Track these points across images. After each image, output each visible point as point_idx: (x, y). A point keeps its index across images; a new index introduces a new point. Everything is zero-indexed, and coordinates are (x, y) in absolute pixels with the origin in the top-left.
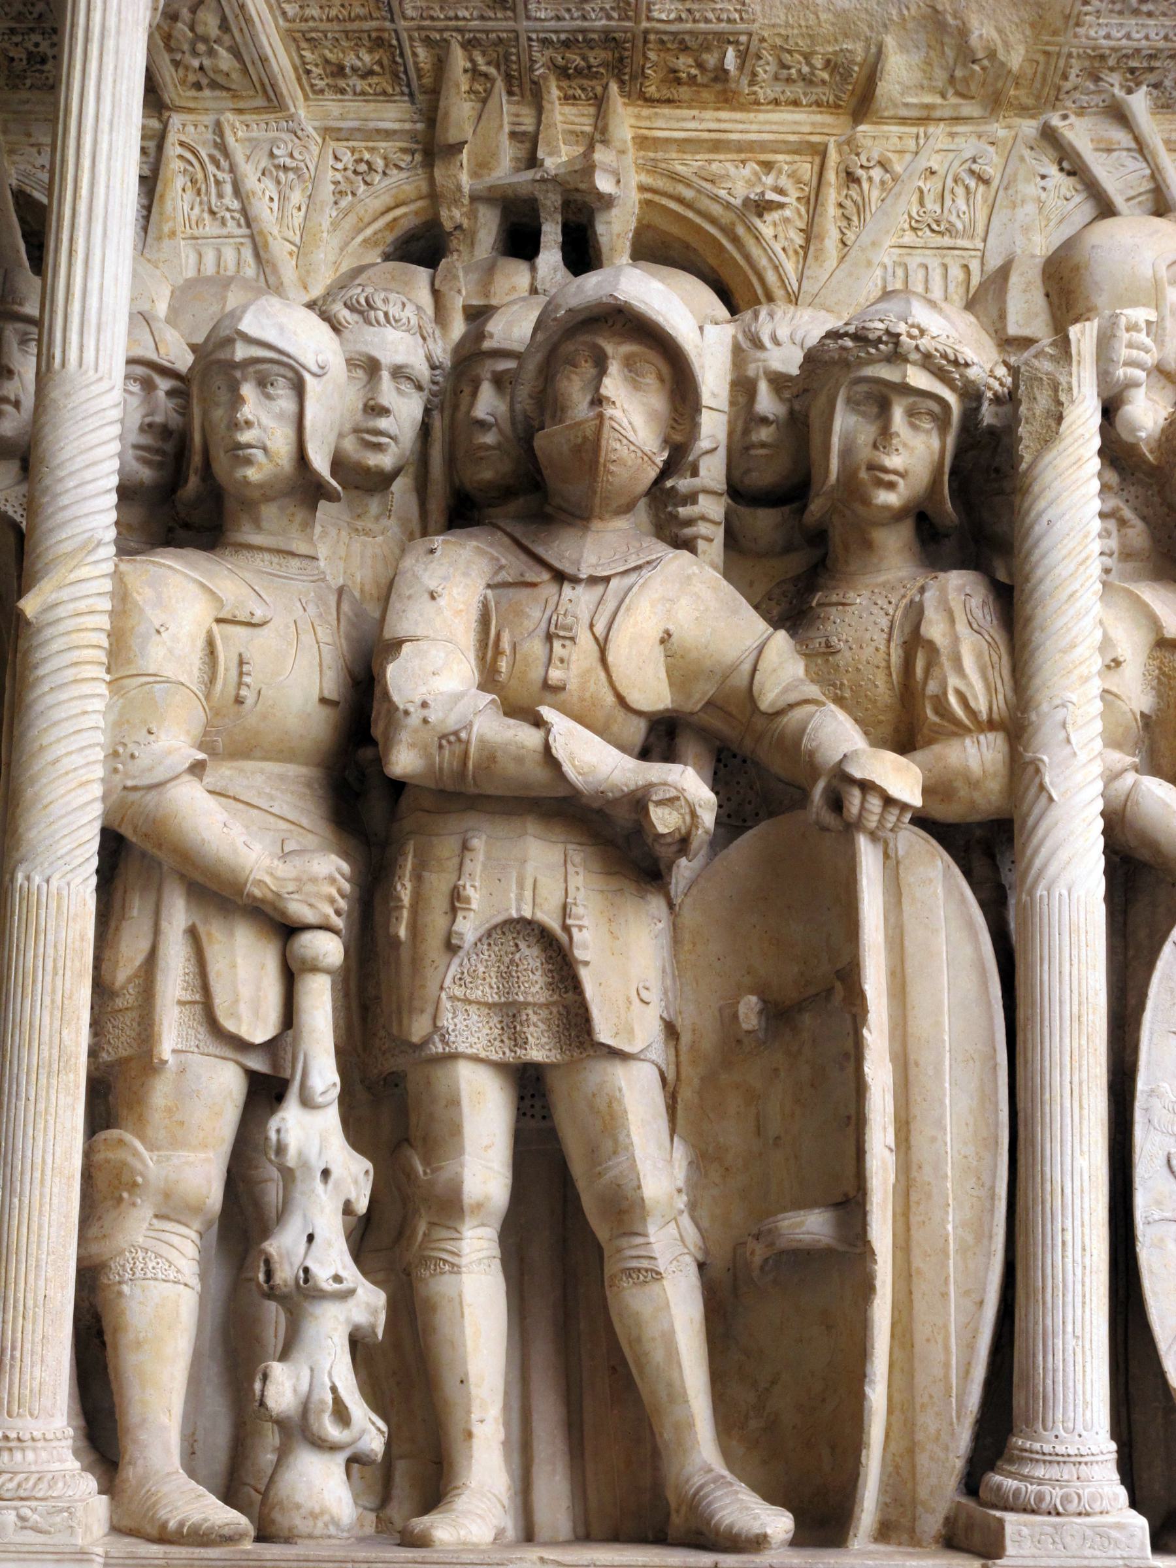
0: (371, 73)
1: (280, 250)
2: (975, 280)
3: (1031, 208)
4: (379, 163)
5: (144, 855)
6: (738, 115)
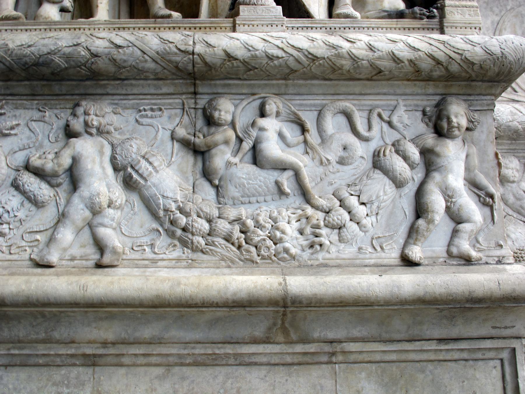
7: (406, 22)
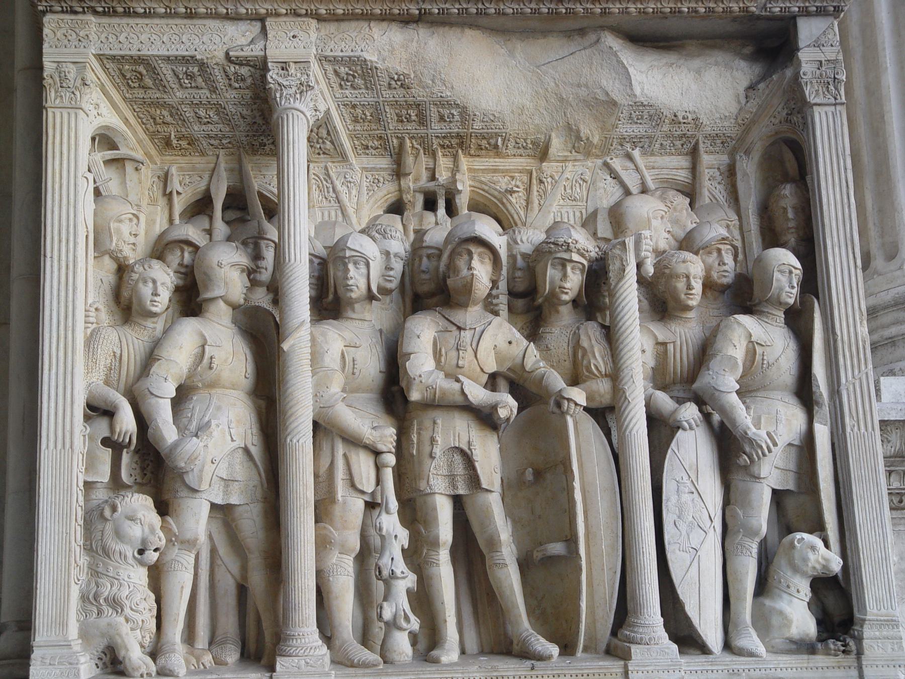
0: (378, 148)
1: (351, 211)
2: (584, 217)
3: (602, 191)
4: (381, 180)
5: (325, 428)
6: (502, 160)
7: (820, 660)
